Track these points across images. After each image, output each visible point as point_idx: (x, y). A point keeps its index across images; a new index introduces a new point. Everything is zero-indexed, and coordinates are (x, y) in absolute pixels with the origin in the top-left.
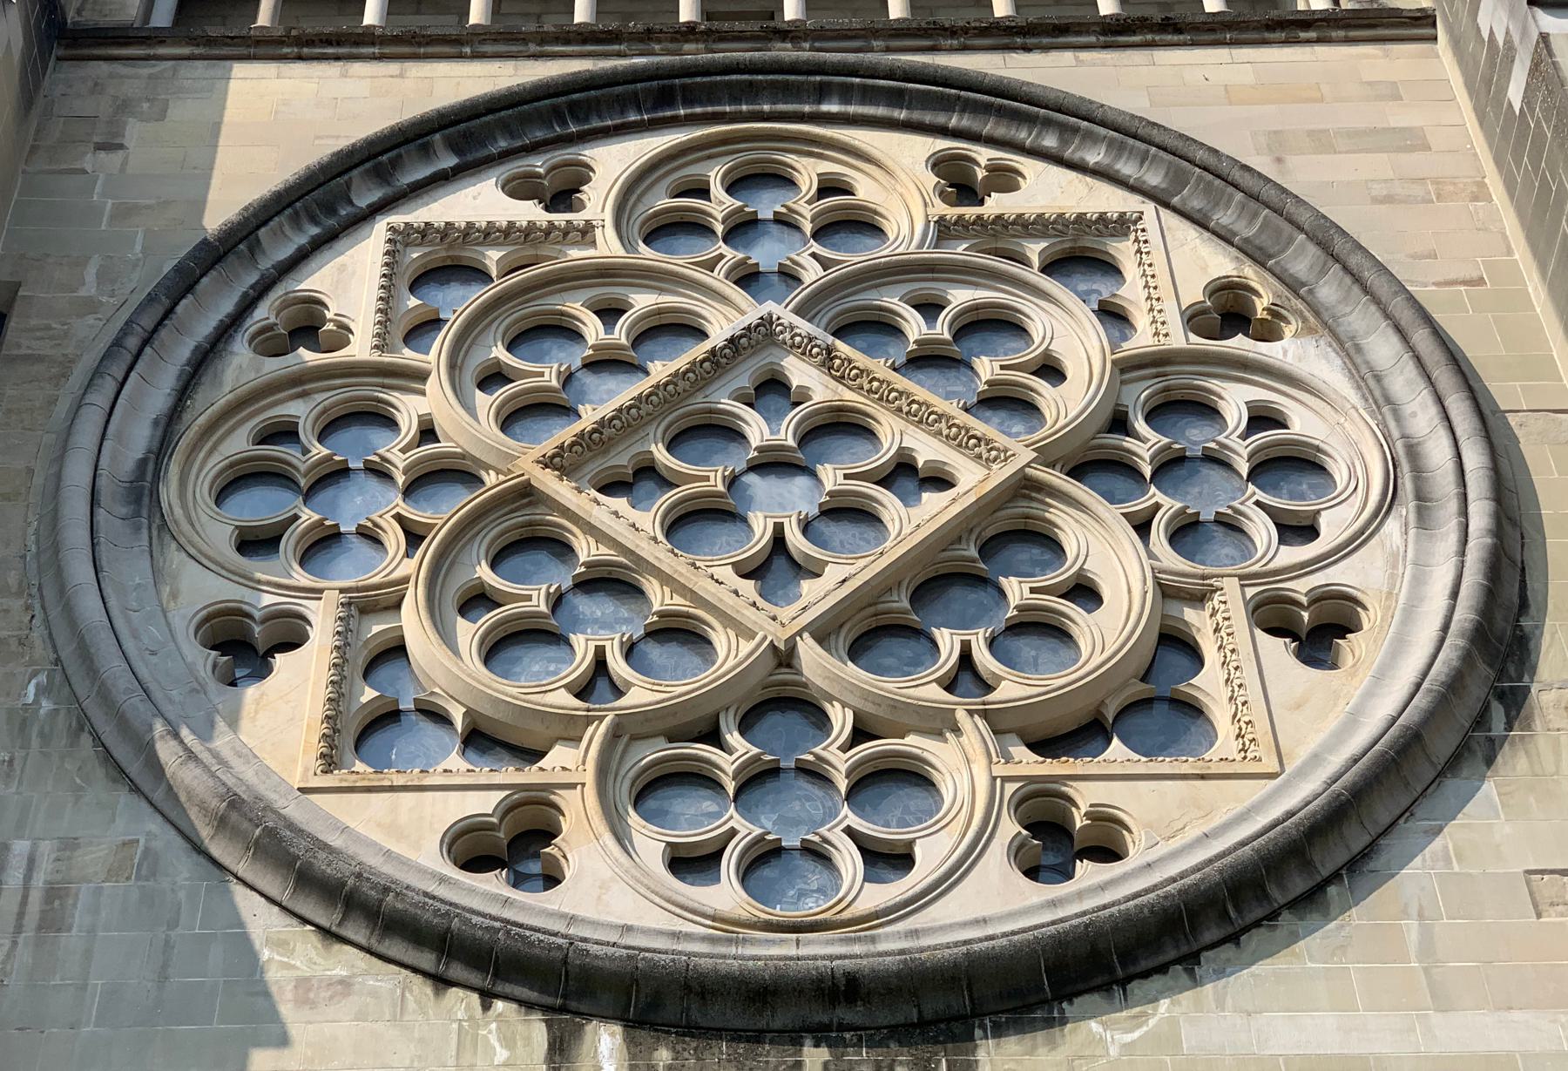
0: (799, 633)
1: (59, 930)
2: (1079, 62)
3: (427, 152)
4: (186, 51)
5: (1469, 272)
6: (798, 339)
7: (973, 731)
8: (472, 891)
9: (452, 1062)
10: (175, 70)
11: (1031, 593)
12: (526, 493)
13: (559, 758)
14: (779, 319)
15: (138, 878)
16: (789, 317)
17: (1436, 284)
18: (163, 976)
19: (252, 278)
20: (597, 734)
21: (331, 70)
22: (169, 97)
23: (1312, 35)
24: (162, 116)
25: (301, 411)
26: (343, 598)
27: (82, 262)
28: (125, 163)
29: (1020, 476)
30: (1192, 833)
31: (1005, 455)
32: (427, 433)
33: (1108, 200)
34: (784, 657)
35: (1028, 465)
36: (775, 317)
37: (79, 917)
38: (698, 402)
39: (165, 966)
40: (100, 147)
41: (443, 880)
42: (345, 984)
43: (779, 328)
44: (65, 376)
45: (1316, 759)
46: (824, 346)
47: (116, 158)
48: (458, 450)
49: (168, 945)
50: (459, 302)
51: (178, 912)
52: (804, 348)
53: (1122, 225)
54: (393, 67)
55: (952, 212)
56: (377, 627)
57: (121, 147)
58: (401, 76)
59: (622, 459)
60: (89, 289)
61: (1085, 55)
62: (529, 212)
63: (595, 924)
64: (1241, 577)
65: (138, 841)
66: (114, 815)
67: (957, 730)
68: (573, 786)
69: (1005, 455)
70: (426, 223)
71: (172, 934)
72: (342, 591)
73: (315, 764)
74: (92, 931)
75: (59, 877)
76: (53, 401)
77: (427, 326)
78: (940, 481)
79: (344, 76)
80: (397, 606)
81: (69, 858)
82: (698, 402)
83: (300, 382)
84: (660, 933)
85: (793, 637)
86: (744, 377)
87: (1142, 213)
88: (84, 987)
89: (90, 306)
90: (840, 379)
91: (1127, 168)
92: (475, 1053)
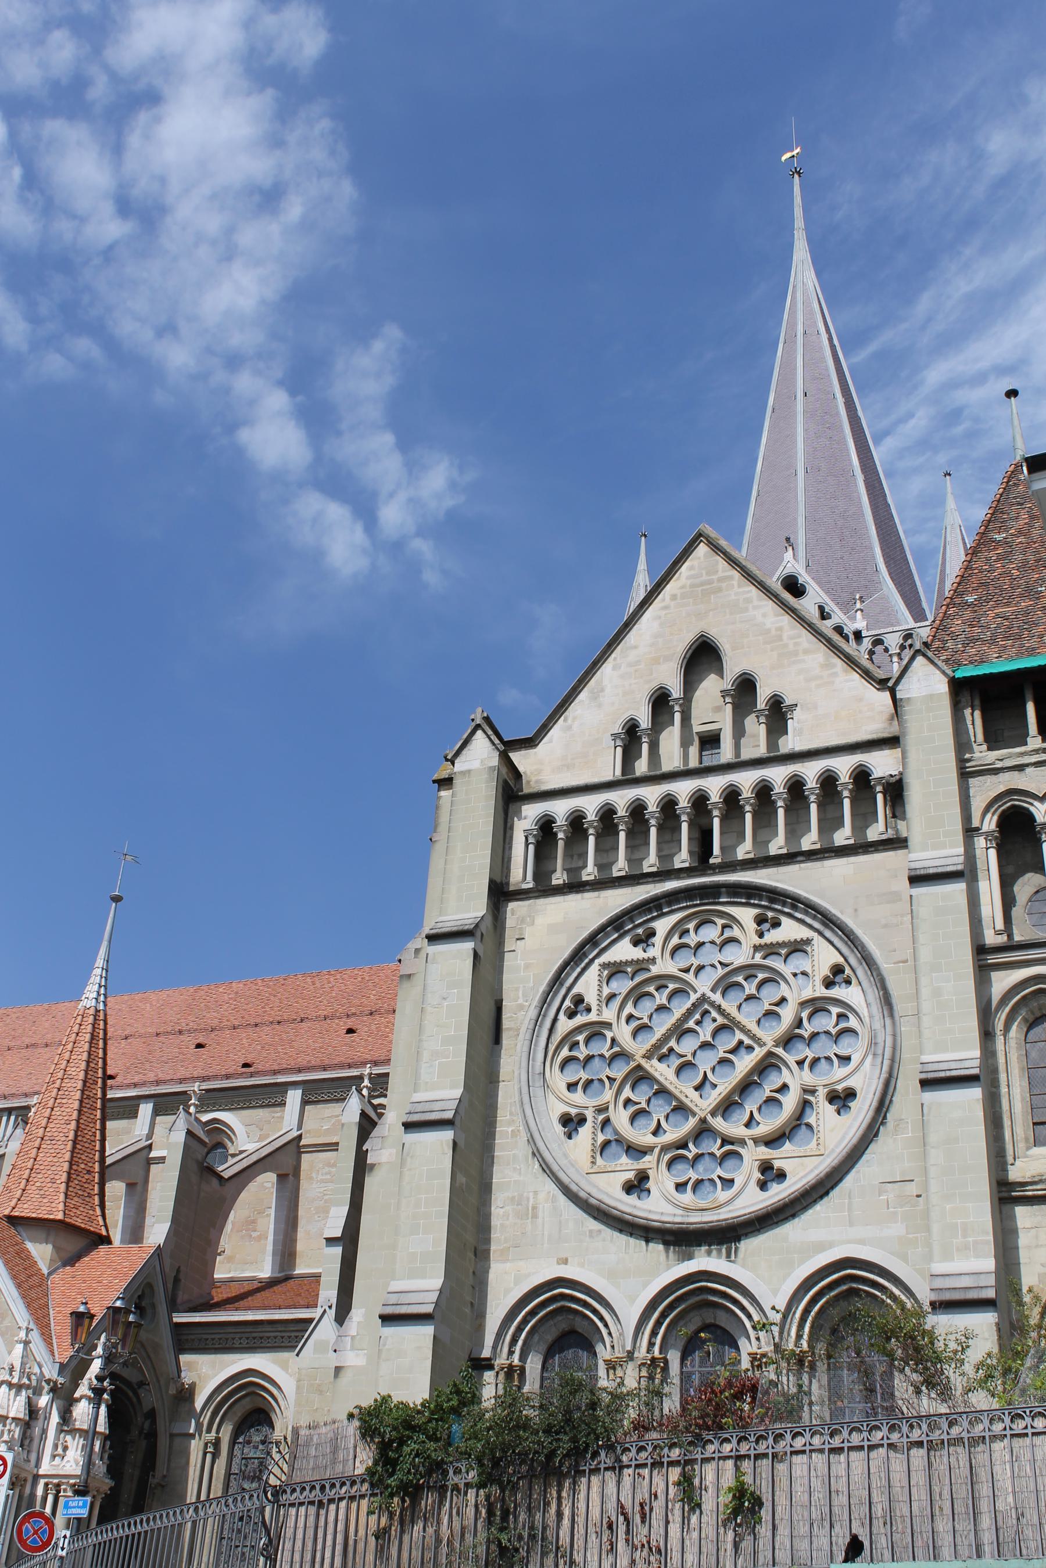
2: (800, 868)
3: (607, 936)
4: (537, 894)
5: (904, 958)
7: (750, 1143)
8: (627, 1204)
12: (639, 1067)
13: (647, 1158)
16: (709, 994)
17: (894, 963)
18: (560, 1231)
20: (657, 1151)
21: (579, 896)
24: (533, 923)
25: (581, 1038)
27: (517, 989)
30: (802, 1174)
31: (765, 1044)
32: (613, 1040)
33: (803, 933)
37: (540, 1214)
40: (518, 939)
41: (620, 1201)
42: (600, 1231)
45: (833, 1150)
49: (560, 1222)
50: (622, 986)
53: (808, 942)
54: (596, 894)
55: (757, 941)
59: (665, 1050)
60: (520, 1001)
61: (802, 865)
69: (765, 1044)
73: (590, 1165)
77: (612, 996)
78: (750, 1048)
79: (583, 899)
80: (607, 1108)
83: (578, 1029)
84: (670, 1215)
89: (521, 1007)
91: (809, 920)
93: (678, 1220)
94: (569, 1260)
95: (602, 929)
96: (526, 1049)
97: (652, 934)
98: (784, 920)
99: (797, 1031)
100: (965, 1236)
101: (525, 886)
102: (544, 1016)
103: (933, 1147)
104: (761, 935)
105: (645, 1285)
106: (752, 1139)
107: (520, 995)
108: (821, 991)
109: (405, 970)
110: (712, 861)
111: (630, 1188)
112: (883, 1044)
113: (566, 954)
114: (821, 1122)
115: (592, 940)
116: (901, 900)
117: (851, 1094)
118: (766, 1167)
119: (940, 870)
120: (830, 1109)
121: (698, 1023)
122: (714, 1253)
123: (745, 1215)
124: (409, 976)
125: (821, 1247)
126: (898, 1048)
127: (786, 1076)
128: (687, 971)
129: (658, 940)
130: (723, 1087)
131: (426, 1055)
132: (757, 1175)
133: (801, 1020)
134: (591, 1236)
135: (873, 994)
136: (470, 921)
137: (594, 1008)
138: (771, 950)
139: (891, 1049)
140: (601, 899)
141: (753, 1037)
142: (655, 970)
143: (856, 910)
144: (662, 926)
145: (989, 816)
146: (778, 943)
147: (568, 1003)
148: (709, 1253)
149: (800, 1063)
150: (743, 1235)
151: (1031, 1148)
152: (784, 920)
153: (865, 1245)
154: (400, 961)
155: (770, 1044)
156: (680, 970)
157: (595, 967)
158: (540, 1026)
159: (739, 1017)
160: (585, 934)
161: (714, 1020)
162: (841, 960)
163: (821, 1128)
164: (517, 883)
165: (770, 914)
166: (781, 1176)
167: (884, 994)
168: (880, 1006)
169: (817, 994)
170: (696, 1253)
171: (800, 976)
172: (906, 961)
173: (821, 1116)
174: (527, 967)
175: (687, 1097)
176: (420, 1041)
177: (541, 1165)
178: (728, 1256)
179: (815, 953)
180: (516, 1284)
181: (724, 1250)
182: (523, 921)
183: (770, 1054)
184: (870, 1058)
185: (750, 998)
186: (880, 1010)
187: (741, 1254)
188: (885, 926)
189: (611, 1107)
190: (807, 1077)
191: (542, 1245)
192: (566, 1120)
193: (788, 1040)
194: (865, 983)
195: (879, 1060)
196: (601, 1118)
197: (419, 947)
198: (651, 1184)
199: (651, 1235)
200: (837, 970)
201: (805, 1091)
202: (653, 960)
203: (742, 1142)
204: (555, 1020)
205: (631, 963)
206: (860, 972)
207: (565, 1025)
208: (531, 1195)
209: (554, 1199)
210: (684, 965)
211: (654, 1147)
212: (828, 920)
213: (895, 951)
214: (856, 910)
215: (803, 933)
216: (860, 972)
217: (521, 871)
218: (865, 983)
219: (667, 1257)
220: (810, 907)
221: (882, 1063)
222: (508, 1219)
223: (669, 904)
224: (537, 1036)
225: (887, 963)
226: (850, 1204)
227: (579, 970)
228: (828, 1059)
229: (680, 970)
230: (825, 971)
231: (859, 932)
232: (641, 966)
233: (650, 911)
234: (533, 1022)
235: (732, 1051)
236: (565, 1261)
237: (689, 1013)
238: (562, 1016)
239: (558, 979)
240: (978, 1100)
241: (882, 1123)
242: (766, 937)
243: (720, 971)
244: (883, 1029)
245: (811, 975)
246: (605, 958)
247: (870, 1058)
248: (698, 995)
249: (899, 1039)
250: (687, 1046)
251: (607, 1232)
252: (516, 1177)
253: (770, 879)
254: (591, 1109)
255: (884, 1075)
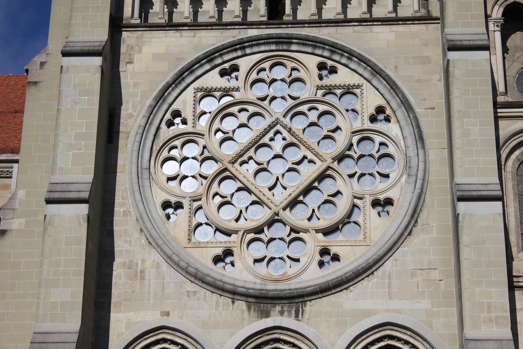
0: (280, 210)
1: (144, 280)
5: (432, 106)
6: (284, 125)
9: (215, 309)
10: (142, 35)
11: (328, 196)
14: (280, 119)
15: (157, 268)
16: (282, 119)
17: (425, 109)
19: (165, 106)
20: (241, 233)
21: (178, 34)
22: (142, 44)
23: (410, 22)
24: (140, 51)
26: (190, 199)
28: (134, 67)
29: (327, 166)
30: (352, 259)
33: (355, 79)
34: (277, 214)
35: (329, 164)
36: (279, 118)
37: (147, 277)
38: (262, 141)
39: (163, 288)
42: (195, 292)
43: (280, 121)
44: (128, 137)
46: (289, 127)
47: (132, 65)
48: (211, 155)
49: (163, 282)
51: (165, 276)
52: (285, 127)
53: (358, 86)
55: (320, 83)
56: (196, 204)
57: (132, 63)
58: (194, 36)
59: (245, 158)
61: (356, 28)
62: (223, 82)
63: (240, 280)
64: (370, 195)
65: (156, 260)
66: (151, 254)
67: (309, 232)
68: (236, 247)
70: (202, 87)
71: (164, 281)
72: (190, 197)
73: (186, 241)
74: (150, 280)
75: (142, 268)
76: (127, 145)
79: (181, 36)
81: (144, 264)
82: (262, 141)
85: (279, 211)
86: (271, 134)
87: (363, 84)
88: (149, 292)
90: (292, 135)
91: (360, 70)
92: (219, 307)
93: (258, 287)
94: (171, 313)
95: (198, 62)
96: (136, 148)
97: (235, 68)
98: (339, 67)
99: (348, 153)
100: (489, 312)
101: (133, 22)
102: (150, 124)
103: (465, 246)
104: (321, 78)
105: (231, 335)
106: (315, 230)
107: (130, 106)
108: (368, 125)
109: (31, 78)
110: (285, 18)
111: (217, 260)
112: (416, 168)
113: (169, 78)
114: (368, 221)
115: (190, 69)
116: (430, 62)
117: (389, 202)
118: (324, 252)
119: (471, 43)
120: (374, 212)
121: (272, 139)
122: (286, 313)
123: (311, 286)
124: (36, 83)
125: (368, 313)
126: (427, 172)
127: (340, 184)
128: (263, 99)
129: (242, 73)
130: (292, 190)
131: (61, 146)
132: (318, 258)
133: (352, 145)
134: (188, 296)
135: (409, 131)
136: (97, 44)
137: (190, 121)
138: (329, 90)
139: (423, 172)
140: (196, 38)
141: (316, 155)
142: (238, 96)
143: (396, 67)
144: (245, 64)
145: (496, 7)
146: (335, 86)
147: (168, 116)
148: (282, 313)
149: (351, 176)
150: (308, 301)
151: (520, 252)
152: (339, 67)
153: (401, 314)
154: (27, 71)
155: (330, 161)
156: (258, 99)
157: (191, 89)
158: (147, 132)
159: (305, 137)
160: (184, 64)
161: (284, 139)
162: (383, 102)
163: (368, 226)
164: (127, 19)
165: (330, 63)
166: (336, 258)
167: (418, 131)
168: (414, 140)
169: (366, 127)
170: (272, 313)
171: (350, 112)
172: (433, 108)
173: (367, 217)
174: (136, 85)
175: (264, 195)
176: (56, 135)
177: (147, 239)
178: (297, 316)
179: (364, 95)
180: (127, 329)
181: (293, 312)
182: (132, 48)
183: (328, 168)
184: (405, 177)
185: (312, 124)
186: (415, 143)
187: (306, 316)
188: (418, 81)
189: (204, 198)
190: (356, 186)
191: (149, 300)
192: (166, 205)
193: (340, 158)
194: (403, 122)
195: (413, 179)
196: (196, 204)
197: (44, 60)
198: (235, 258)
199: (237, 297)
200: (380, 110)
201: (355, 197)
202: (237, 90)
203: (306, 231)
204: (158, 128)
205: (220, 90)
206: (399, 113)
207: (166, 133)
208: (140, 262)
209: (158, 266)
210: (261, 94)
211: (238, 231)
212: (377, 71)
213: (425, 100)
214: (396, 67)
215: (355, 79)
216: (399, 113)
217: (130, 9)
218: (403, 122)
219: (250, 314)
220: (362, 60)
221: (416, 181)
222: (120, 279)
223: (251, 46)
224: (145, 139)
225: (419, 109)
226: (390, 284)
227: (177, 91)
228: (371, 175)
229: (258, 99)
230: (372, 110)
231: (399, 83)
232: (226, 92)
233: (236, 50)
234: (142, 128)
235: (299, 163)
236: (168, 314)
237: (266, 132)
238: (163, 126)
239: (161, 96)
240: (500, 214)
241: (414, 226)
242: (324, 81)
243: (291, 102)
244: (416, 157)
245: (360, 113)
246: (198, 84)
247: (405, 177)
248: (273, 119)
249: (427, 165)
250: (263, 155)
251: (203, 292)
252: (127, 247)
253: (331, 37)
254: (188, 199)
255: (418, 191)
